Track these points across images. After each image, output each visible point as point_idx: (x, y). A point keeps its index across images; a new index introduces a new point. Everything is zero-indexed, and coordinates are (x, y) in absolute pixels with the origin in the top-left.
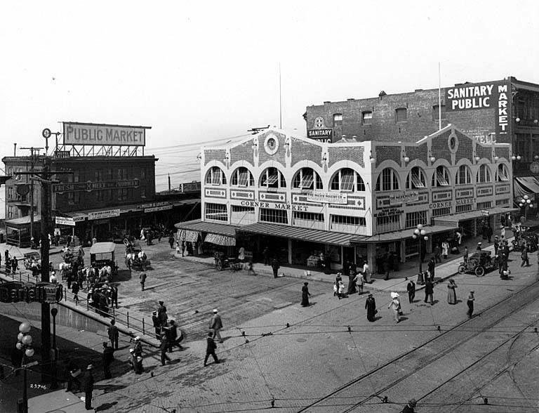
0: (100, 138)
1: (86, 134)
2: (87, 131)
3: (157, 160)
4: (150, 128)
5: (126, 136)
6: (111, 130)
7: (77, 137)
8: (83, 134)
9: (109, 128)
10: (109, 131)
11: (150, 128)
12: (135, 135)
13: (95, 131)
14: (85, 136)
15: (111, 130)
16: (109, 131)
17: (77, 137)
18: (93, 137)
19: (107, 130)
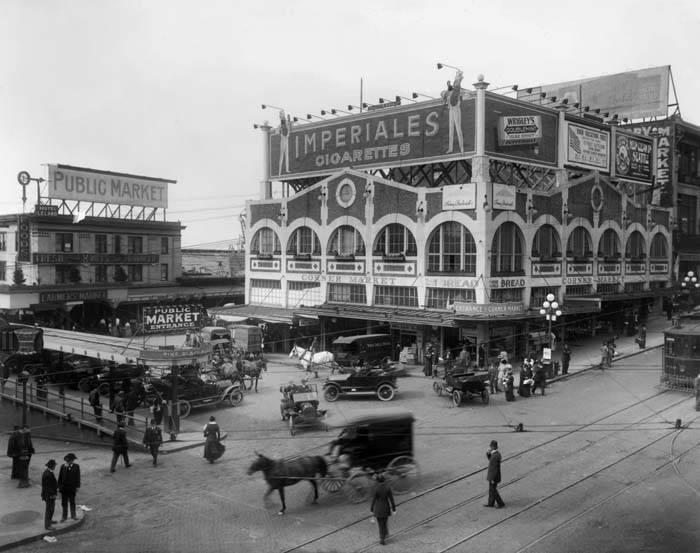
0: (102, 191)
1: (82, 184)
2: (83, 181)
5: (140, 192)
6: (119, 181)
7: (70, 187)
8: (77, 183)
10: (116, 183)
13: (95, 181)
14: (80, 188)
15: (119, 181)
16: (116, 183)
18: (91, 189)
19: (113, 182)
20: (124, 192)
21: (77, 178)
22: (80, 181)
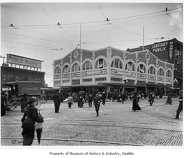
3: (45, 73)
4: (43, 61)
5: (33, 63)
6: (27, 60)
7: (13, 60)
9: (26, 59)
10: (26, 60)
11: (43, 61)
12: (37, 64)
14: (16, 61)
15: (27, 60)
17: (13, 60)
18: (19, 61)
19: (25, 60)
20: (29, 63)
21: (15, 58)
22: (16, 59)
